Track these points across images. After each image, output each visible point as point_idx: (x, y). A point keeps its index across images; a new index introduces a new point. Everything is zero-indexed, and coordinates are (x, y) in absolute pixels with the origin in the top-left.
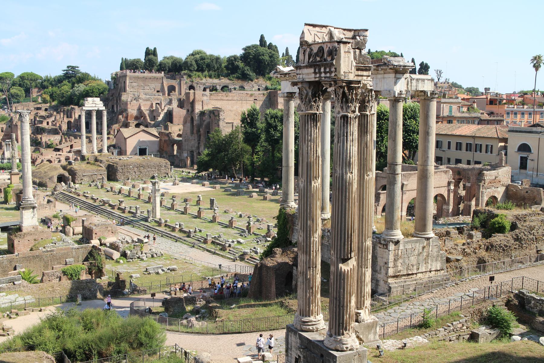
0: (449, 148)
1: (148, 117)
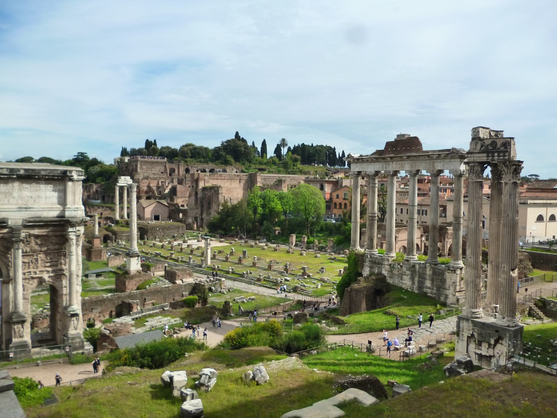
0: (402, 213)
1: (156, 192)
